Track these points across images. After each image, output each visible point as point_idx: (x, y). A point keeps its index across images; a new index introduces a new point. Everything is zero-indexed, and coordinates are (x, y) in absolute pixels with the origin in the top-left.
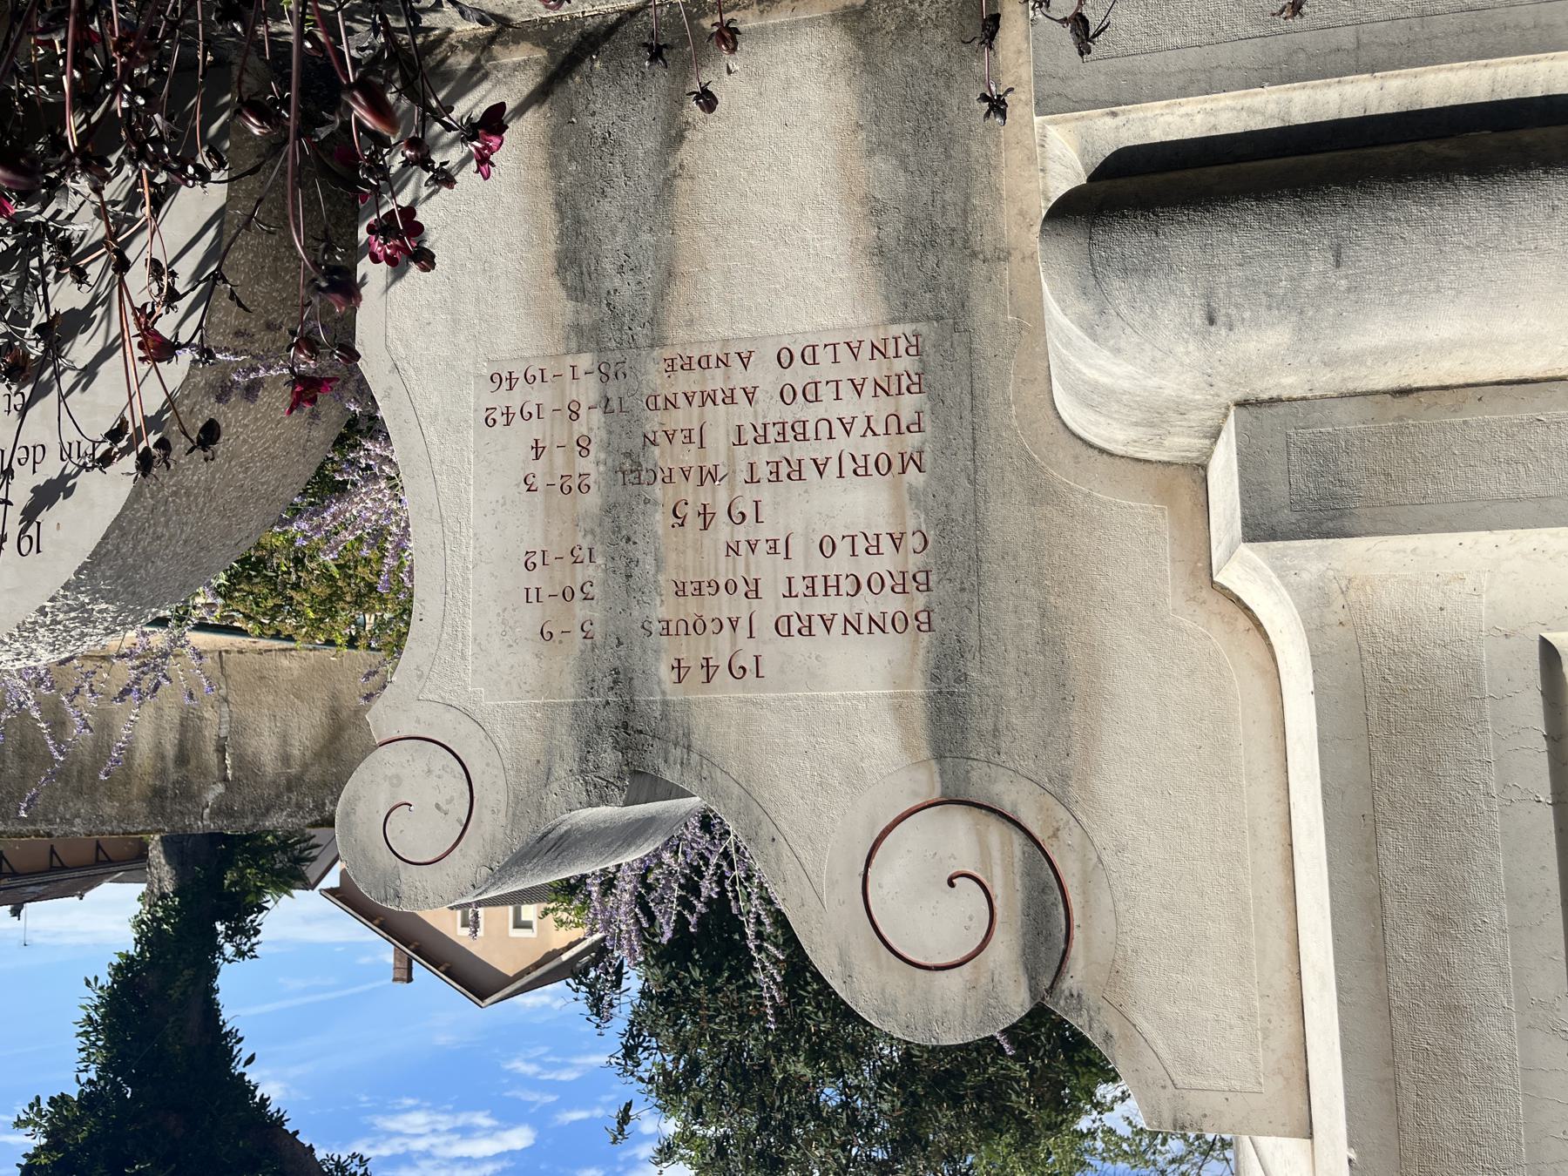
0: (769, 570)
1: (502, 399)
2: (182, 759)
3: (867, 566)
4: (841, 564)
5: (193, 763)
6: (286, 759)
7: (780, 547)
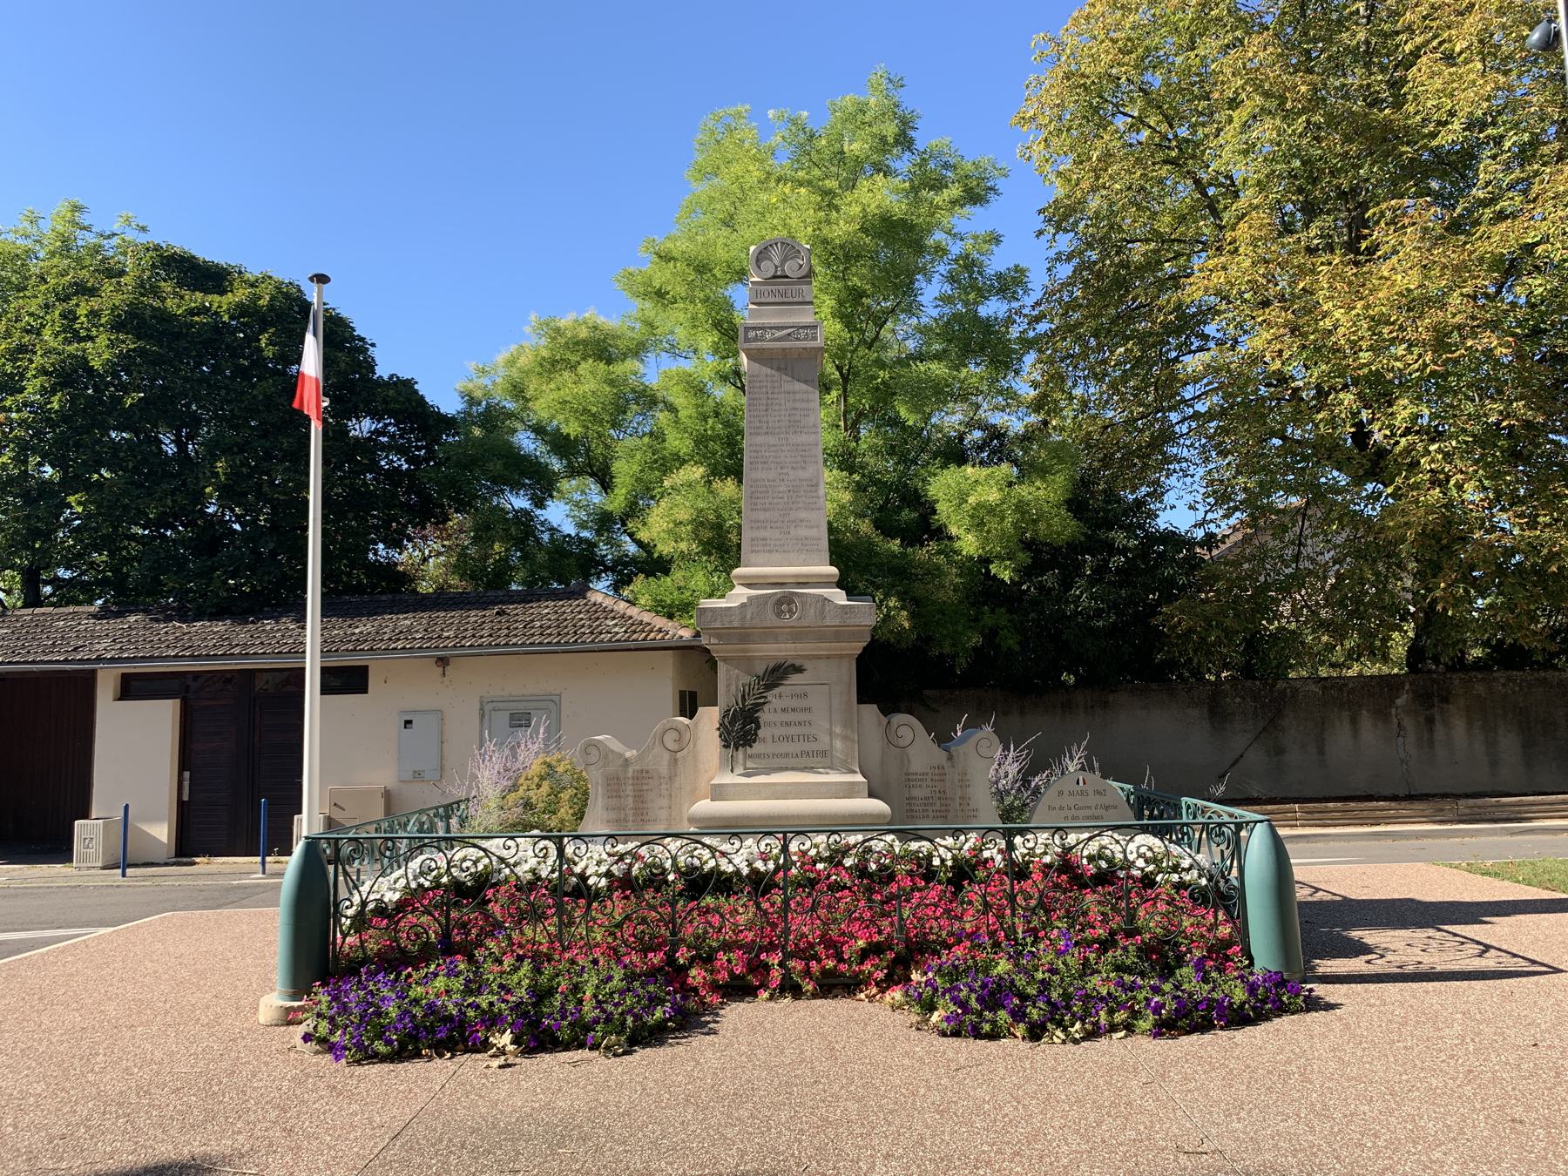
0: (931, 784)
2: (1430, 721)
5: (1422, 719)
6: (1354, 721)
7: (928, 786)
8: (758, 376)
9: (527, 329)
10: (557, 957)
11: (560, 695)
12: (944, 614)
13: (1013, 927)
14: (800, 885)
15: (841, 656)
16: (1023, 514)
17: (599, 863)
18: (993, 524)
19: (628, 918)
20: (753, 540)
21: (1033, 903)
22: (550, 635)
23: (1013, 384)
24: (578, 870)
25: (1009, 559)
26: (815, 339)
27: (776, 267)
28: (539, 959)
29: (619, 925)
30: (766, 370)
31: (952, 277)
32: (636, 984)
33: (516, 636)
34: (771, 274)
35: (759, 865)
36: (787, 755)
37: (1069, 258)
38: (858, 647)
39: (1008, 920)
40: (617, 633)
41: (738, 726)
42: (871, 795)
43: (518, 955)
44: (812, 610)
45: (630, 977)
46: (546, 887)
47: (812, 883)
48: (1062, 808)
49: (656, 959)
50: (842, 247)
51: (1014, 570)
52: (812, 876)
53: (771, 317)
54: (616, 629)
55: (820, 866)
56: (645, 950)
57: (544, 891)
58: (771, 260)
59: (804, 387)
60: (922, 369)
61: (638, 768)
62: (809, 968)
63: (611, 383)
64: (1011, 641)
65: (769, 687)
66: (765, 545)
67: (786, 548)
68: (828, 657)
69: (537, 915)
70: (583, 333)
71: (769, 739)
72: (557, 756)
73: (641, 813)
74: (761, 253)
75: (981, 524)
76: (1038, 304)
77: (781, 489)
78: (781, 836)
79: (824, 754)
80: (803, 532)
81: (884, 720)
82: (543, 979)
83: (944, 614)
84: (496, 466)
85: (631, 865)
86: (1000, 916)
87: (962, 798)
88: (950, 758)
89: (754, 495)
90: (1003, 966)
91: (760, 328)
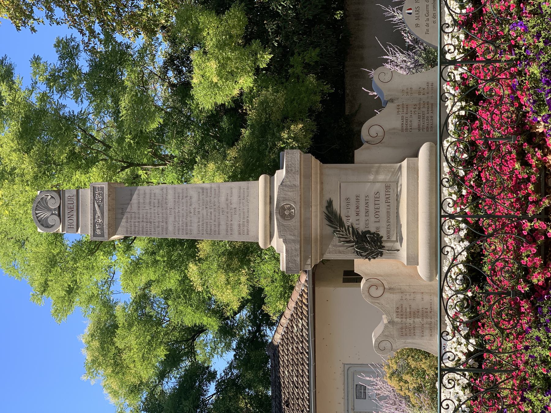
1: (430, 84)
3: (408, 125)
4: (409, 123)
8: (127, 228)
9: (93, 382)
10: (523, 374)
11: (344, 364)
12: (294, 100)
13: (508, 61)
14: (477, 207)
15: (321, 174)
16: (225, 45)
17: (460, 344)
18: (232, 66)
19: (497, 325)
20: (240, 234)
21: (492, 47)
22: (303, 370)
23: (136, 49)
24: (463, 358)
25: (256, 54)
26: (102, 189)
27: (52, 214)
28: (525, 387)
29: (502, 331)
30: (123, 223)
31: (61, 90)
32: (542, 320)
33: (303, 394)
34: (57, 218)
35: (462, 234)
36: (388, 213)
37: (50, 9)
38: (315, 162)
39: (503, 65)
40: (303, 325)
41: (368, 246)
42: (416, 155)
43: (521, 401)
44: (289, 193)
45: (537, 324)
46: (475, 380)
47: (476, 198)
48: (427, 25)
49: (525, 306)
50: (39, 166)
51: (264, 52)
52: (470, 198)
53: (87, 219)
54: (300, 325)
55: (464, 192)
56: (519, 313)
57: (478, 381)
58: (48, 217)
59: (135, 197)
60: (124, 112)
61: (395, 315)
62: (533, 202)
63: (131, 325)
64: (313, 55)
65: (342, 224)
67: (246, 210)
68: (322, 183)
69: (494, 387)
70: (96, 344)
71: (377, 225)
72: (385, 369)
73: (425, 313)
74: (42, 225)
75: (232, 73)
76: (81, 31)
77: (205, 214)
78: (443, 219)
79: (388, 187)
80: (235, 199)
81: (365, 145)
82: (538, 384)
83: (294, 100)
84: (187, 405)
85: (461, 322)
86: (501, 70)
87: (419, 93)
88: (392, 101)
89: (209, 233)
90: (535, 69)
91: (94, 226)
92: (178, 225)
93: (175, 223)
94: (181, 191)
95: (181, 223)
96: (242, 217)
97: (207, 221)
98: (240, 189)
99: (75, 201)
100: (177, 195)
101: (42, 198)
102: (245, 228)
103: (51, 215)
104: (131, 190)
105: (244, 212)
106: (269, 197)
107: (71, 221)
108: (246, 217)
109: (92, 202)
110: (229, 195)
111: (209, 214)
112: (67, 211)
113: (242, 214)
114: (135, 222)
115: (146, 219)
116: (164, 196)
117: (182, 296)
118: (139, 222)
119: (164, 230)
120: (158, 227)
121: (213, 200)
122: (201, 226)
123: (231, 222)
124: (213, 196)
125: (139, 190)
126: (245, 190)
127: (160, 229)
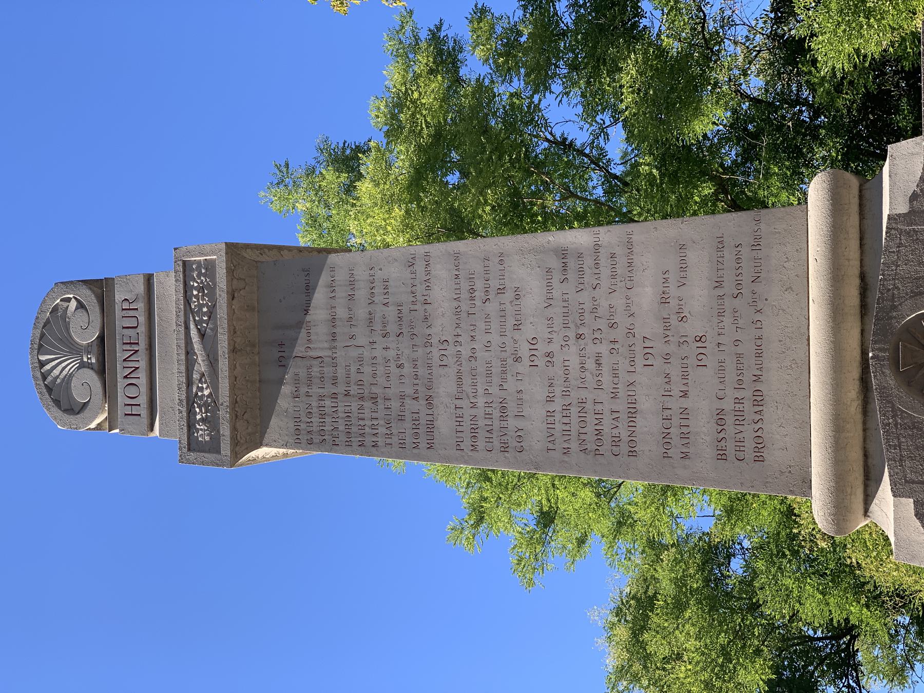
8: (297, 420)
20: (722, 456)
26: (210, 267)
27: (82, 365)
30: (284, 402)
34: (91, 377)
58: (70, 376)
59: (320, 296)
63: (679, 606)
66: (739, 416)
67: (748, 348)
70: (623, 632)
74: (57, 403)
77: (574, 362)
89: (591, 446)
91: (190, 412)
92: (473, 412)
93: (459, 403)
94: (478, 267)
95: (481, 402)
96: (731, 376)
97: (583, 394)
98: (719, 249)
99: (142, 319)
100: (465, 286)
101: (55, 309)
102: (748, 432)
103: (78, 368)
104: (307, 272)
105: (739, 356)
106: (857, 282)
107: (132, 392)
108: (748, 377)
109: (182, 319)
110: (673, 277)
111: (590, 365)
112: (120, 355)
113: (730, 365)
114: (321, 398)
115: (360, 383)
116: (420, 289)
117: (787, 553)
118: (334, 396)
119: (422, 430)
120: (401, 419)
121: (604, 304)
122: (558, 416)
123: (685, 403)
124: (605, 283)
125: (332, 269)
126: (745, 252)
127: (408, 424)
